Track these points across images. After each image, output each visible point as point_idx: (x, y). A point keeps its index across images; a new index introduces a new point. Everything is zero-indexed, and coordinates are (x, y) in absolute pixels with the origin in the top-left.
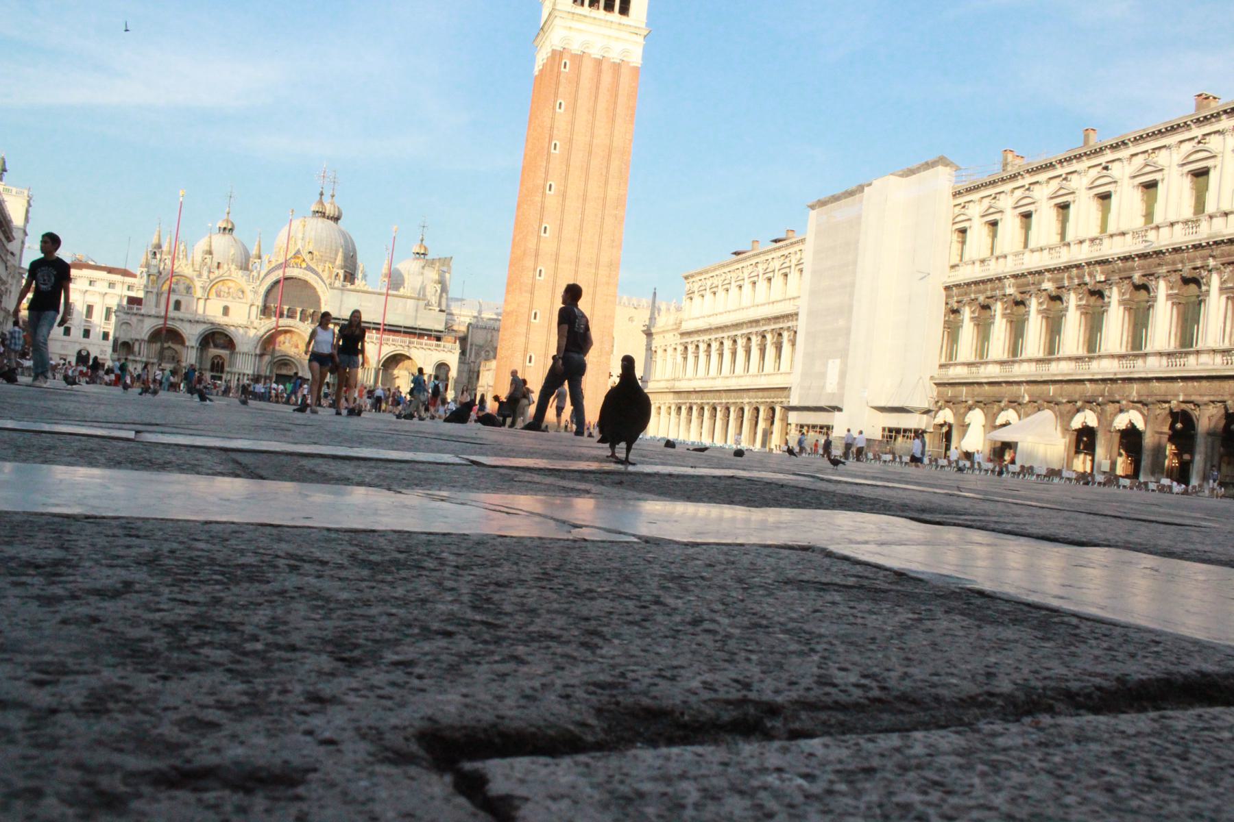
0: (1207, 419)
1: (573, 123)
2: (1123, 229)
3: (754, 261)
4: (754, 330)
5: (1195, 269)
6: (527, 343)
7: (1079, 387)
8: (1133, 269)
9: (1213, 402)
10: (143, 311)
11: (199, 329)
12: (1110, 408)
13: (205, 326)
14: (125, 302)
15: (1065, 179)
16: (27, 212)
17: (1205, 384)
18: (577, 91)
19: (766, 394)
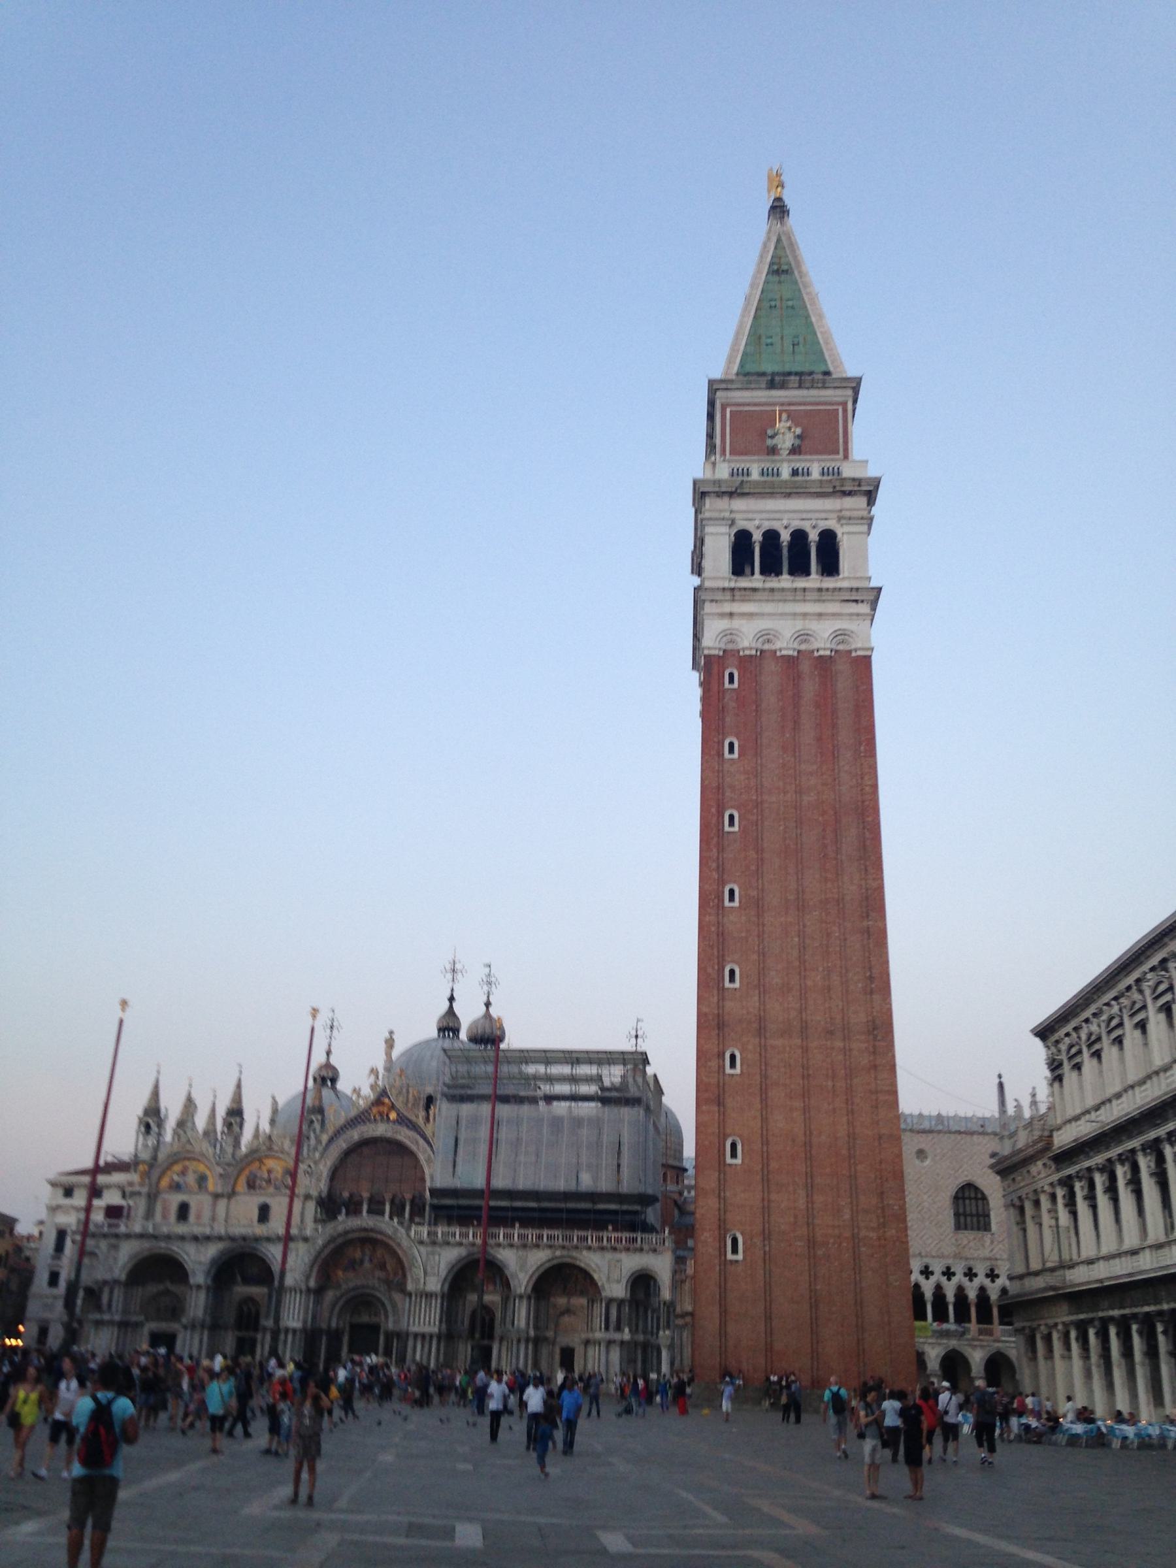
3: (1155, 961)
11: (211, 1251)
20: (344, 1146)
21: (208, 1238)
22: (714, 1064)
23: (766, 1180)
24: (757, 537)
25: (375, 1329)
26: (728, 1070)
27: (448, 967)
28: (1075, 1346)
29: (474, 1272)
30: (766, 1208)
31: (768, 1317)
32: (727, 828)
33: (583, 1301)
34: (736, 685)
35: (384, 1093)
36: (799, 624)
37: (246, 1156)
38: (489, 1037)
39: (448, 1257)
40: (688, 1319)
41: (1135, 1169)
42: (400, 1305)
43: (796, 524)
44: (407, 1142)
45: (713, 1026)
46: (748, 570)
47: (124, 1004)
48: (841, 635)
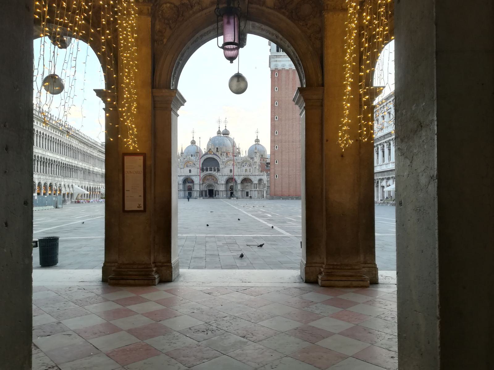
11: (182, 178)
13: (184, 177)
20: (204, 159)
21: (181, 176)
22: (273, 148)
25: (213, 190)
26: (276, 149)
27: (218, 121)
31: (282, 186)
32: (276, 105)
33: (250, 184)
34: (277, 76)
35: (210, 149)
37: (186, 161)
38: (226, 133)
39: (225, 178)
40: (269, 187)
42: (217, 186)
45: (273, 142)
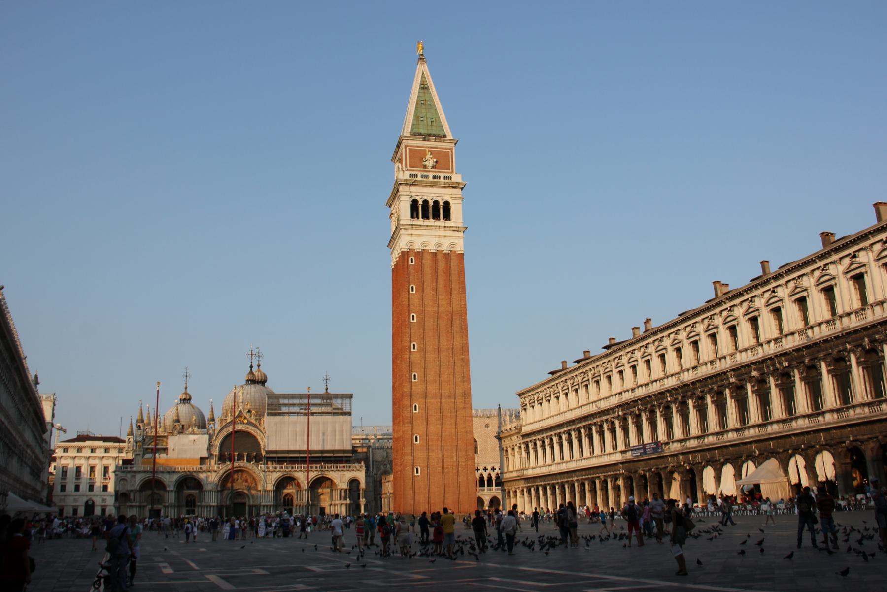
0: (869, 450)
1: (423, 299)
2: (792, 330)
3: (563, 379)
4: (572, 427)
5: (840, 351)
6: (413, 460)
7: (788, 440)
8: (803, 356)
9: (871, 438)
10: (134, 469)
11: (175, 477)
12: (810, 452)
14: (121, 462)
15: (751, 301)
16: (53, 410)
17: (863, 427)
18: (422, 277)
19: (588, 472)
23: (428, 449)
24: (420, 203)
25: (244, 504)
28: (526, 494)
29: (285, 481)
30: (428, 458)
31: (429, 493)
33: (329, 490)
36: (437, 240)
39: (275, 476)
41: (552, 440)
43: (436, 199)
44: (252, 432)
46: (415, 214)
47: (159, 383)
48: (452, 244)
